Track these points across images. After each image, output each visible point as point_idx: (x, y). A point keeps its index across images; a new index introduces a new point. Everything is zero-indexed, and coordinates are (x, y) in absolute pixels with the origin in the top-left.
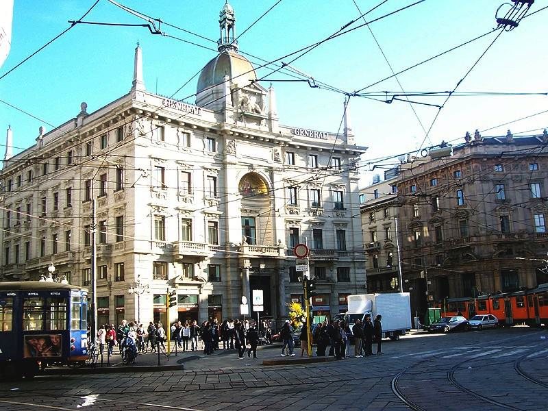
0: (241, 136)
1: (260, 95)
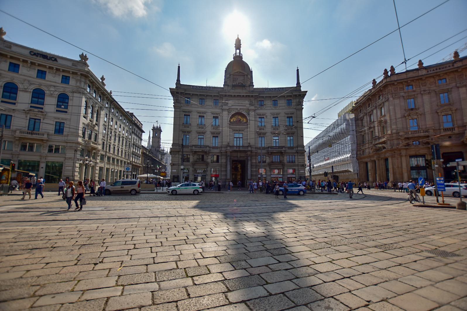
1: (244, 75)
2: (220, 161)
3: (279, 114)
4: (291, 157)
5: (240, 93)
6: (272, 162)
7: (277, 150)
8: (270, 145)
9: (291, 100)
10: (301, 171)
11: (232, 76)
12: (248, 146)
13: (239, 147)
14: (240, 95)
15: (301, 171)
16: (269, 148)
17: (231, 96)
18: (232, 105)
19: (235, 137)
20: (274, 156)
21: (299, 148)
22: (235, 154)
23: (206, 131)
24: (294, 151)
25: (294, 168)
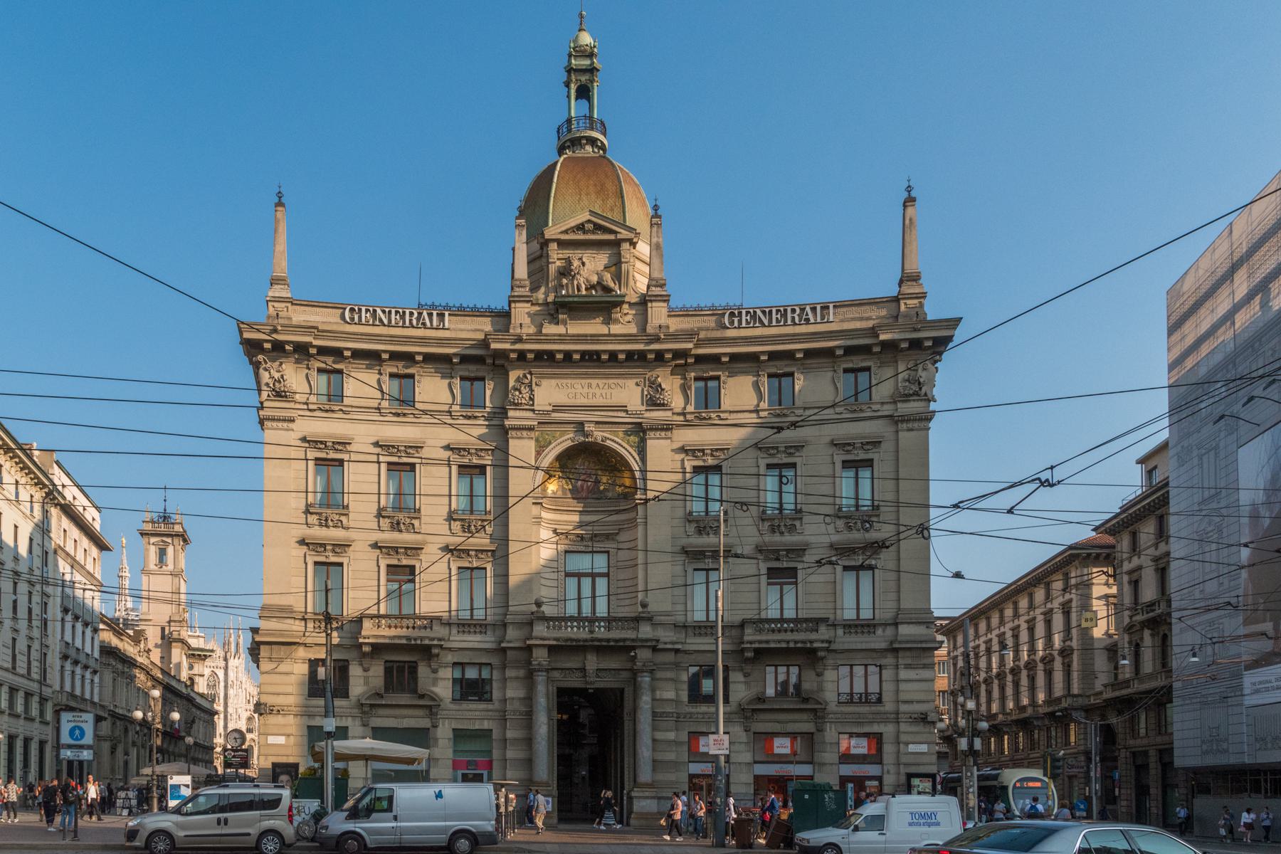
0: (545, 358)
2: (496, 694)
3: (799, 448)
4: (859, 671)
5: (595, 338)
6: (761, 699)
7: (789, 636)
8: (749, 615)
9: (868, 369)
10: (912, 748)
11: (554, 246)
12: (637, 620)
13: (593, 620)
14: (598, 353)
15: (912, 748)
16: (748, 631)
17: (551, 354)
18: (558, 408)
19: (570, 568)
20: (770, 670)
21: (904, 630)
22: (572, 662)
23: (425, 543)
24: (879, 640)
25: (876, 728)
